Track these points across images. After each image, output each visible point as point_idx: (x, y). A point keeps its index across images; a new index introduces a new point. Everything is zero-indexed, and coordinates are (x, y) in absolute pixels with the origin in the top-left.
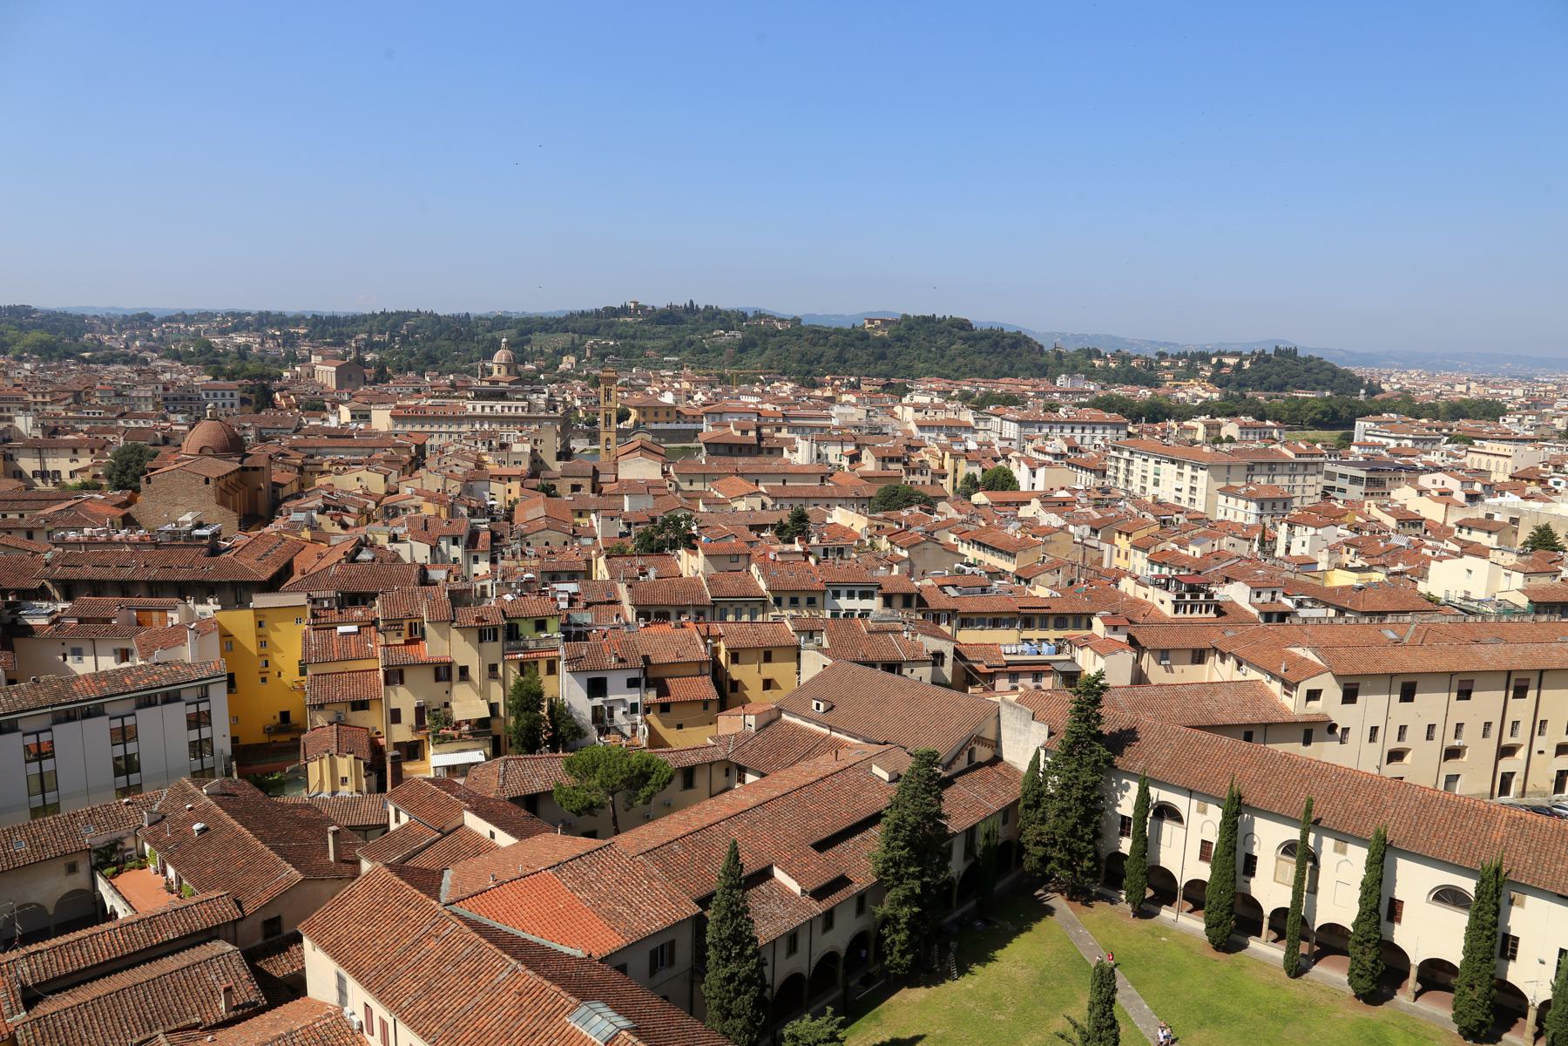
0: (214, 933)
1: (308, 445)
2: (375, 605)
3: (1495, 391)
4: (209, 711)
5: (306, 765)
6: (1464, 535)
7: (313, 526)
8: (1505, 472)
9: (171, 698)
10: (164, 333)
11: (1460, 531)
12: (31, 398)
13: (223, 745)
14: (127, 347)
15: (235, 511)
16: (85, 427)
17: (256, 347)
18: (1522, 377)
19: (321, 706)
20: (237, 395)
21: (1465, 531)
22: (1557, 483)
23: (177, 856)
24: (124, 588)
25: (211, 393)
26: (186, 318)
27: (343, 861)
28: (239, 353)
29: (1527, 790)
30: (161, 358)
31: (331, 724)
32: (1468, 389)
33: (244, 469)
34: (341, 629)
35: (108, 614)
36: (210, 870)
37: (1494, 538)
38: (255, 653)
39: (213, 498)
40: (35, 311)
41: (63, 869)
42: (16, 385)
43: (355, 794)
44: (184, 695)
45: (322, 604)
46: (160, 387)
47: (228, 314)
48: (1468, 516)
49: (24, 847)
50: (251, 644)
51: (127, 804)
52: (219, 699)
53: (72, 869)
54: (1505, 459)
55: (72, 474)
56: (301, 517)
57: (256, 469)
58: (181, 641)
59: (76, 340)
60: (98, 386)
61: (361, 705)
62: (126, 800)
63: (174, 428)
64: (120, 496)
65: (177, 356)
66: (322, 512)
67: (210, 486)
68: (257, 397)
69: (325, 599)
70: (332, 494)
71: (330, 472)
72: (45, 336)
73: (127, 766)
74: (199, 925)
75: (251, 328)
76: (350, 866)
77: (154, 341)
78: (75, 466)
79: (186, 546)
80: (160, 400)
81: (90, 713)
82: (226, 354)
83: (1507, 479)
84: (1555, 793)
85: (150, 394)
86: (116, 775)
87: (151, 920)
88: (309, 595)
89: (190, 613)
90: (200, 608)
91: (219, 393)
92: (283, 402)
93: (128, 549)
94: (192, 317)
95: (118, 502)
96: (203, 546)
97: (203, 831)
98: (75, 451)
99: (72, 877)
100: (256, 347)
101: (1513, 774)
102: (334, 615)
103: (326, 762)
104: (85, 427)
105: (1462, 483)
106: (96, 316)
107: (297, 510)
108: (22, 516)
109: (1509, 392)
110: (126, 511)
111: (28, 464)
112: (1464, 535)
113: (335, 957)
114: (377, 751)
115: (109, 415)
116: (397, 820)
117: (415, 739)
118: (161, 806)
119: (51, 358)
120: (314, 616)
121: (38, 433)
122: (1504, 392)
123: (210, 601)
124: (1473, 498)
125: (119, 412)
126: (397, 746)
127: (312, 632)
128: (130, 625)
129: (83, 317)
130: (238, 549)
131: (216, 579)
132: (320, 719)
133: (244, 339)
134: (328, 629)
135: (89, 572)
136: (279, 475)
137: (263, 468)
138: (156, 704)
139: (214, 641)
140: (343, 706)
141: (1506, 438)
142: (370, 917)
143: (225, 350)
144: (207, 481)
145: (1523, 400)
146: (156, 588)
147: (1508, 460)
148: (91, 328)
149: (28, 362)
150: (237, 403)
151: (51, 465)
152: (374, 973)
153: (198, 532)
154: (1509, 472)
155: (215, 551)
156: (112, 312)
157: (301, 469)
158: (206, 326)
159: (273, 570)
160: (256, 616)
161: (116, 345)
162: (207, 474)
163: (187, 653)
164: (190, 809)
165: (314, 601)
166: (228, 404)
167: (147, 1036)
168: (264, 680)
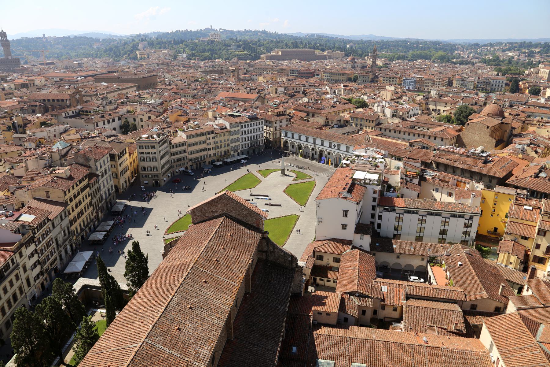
0: (456, 301)
1: (529, 111)
2: (541, 201)
4: (472, 224)
5: (499, 254)
7: (523, 151)
9: (461, 216)
10: (482, 50)
12: (436, 80)
13: (473, 235)
14: (468, 57)
15: (495, 139)
16: (451, 95)
17: (516, 58)
19: (510, 234)
20: (505, 82)
23: (451, 270)
24: (454, 170)
25: (495, 81)
26: (491, 45)
27: (503, 296)
28: (509, 61)
30: (480, 62)
31: (512, 241)
33: (502, 123)
34: (525, 207)
35: (448, 180)
36: (460, 280)
38: (491, 207)
39: (489, 134)
40: (441, 43)
41: (420, 259)
42: (432, 74)
43: (513, 269)
44: (465, 217)
45: (521, 195)
46: (477, 78)
47: (507, 43)
49: (413, 249)
50: (491, 204)
51: (441, 246)
52: (476, 222)
53: (423, 260)
55: (444, 111)
56: (520, 146)
57: (506, 124)
58: (468, 197)
59: (452, 54)
60: (457, 75)
61: (526, 238)
62: (441, 245)
63: (480, 99)
64: (458, 127)
65: (485, 62)
66: (529, 146)
67: (489, 129)
68: (512, 84)
69: (522, 194)
70: (534, 138)
71: (536, 125)
72: (443, 53)
73: (443, 232)
74: (453, 297)
75: (516, 49)
76: (505, 298)
77: (478, 54)
78: (445, 109)
79: (477, 158)
80: (476, 82)
81: (437, 215)
82: (504, 61)
85: (473, 81)
86: (440, 234)
87: (440, 290)
88: (516, 191)
89: (473, 186)
90: (477, 185)
91: (498, 81)
92: (523, 86)
93: (458, 156)
94: (494, 44)
95: (457, 129)
96: (482, 159)
97: (461, 265)
98: (446, 104)
99: (422, 262)
100: (516, 58)
102: (524, 201)
103: (506, 255)
104: (451, 95)
106: (460, 45)
107: (519, 144)
108: (428, 129)
110: (459, 133)
111: (432, 107)
113: (492, 336)
114: (527, 256)
115: (459, 91)
116: (527, 290)
117: (543, 257)
118: (450, 251)
119: (443, 62)
120: (516, 199)
121: (436, 96)
123: (481, 183)
125: (462, 90)
126: (535, 257)
127: (514, 205)
128: (454, 185)
129: (456, 45)
130: (495, 162)
131: (484, 173)
132: (509, 238)
133: (512, 54)
134: (520, 205)
135: (445, 161)
136: (517, 125)
137: (509, 124)
138: (456, 217)
139: (479, 199)
140: (518, 236)
142: (508, 329)
143: (503, 59)
144: (488, 127)
146: (464, 172)
148: (457, 49)
149: (436, 63)
150: (504, 85)
151: (438, 108)
152: (504, 350)
153: (481, 154)
155: (486, 162)
156: (465, 41)
157: (524, 122)
158: (498, 48)
159: (505, 173)
160: (495, 194)
161: (464, 56)
162: (488, 125)
163: (469, 202)
164: (459, 256)
165: (518, 194)
166: (500, 85)
167: (432, 325)
168: (492, 215)
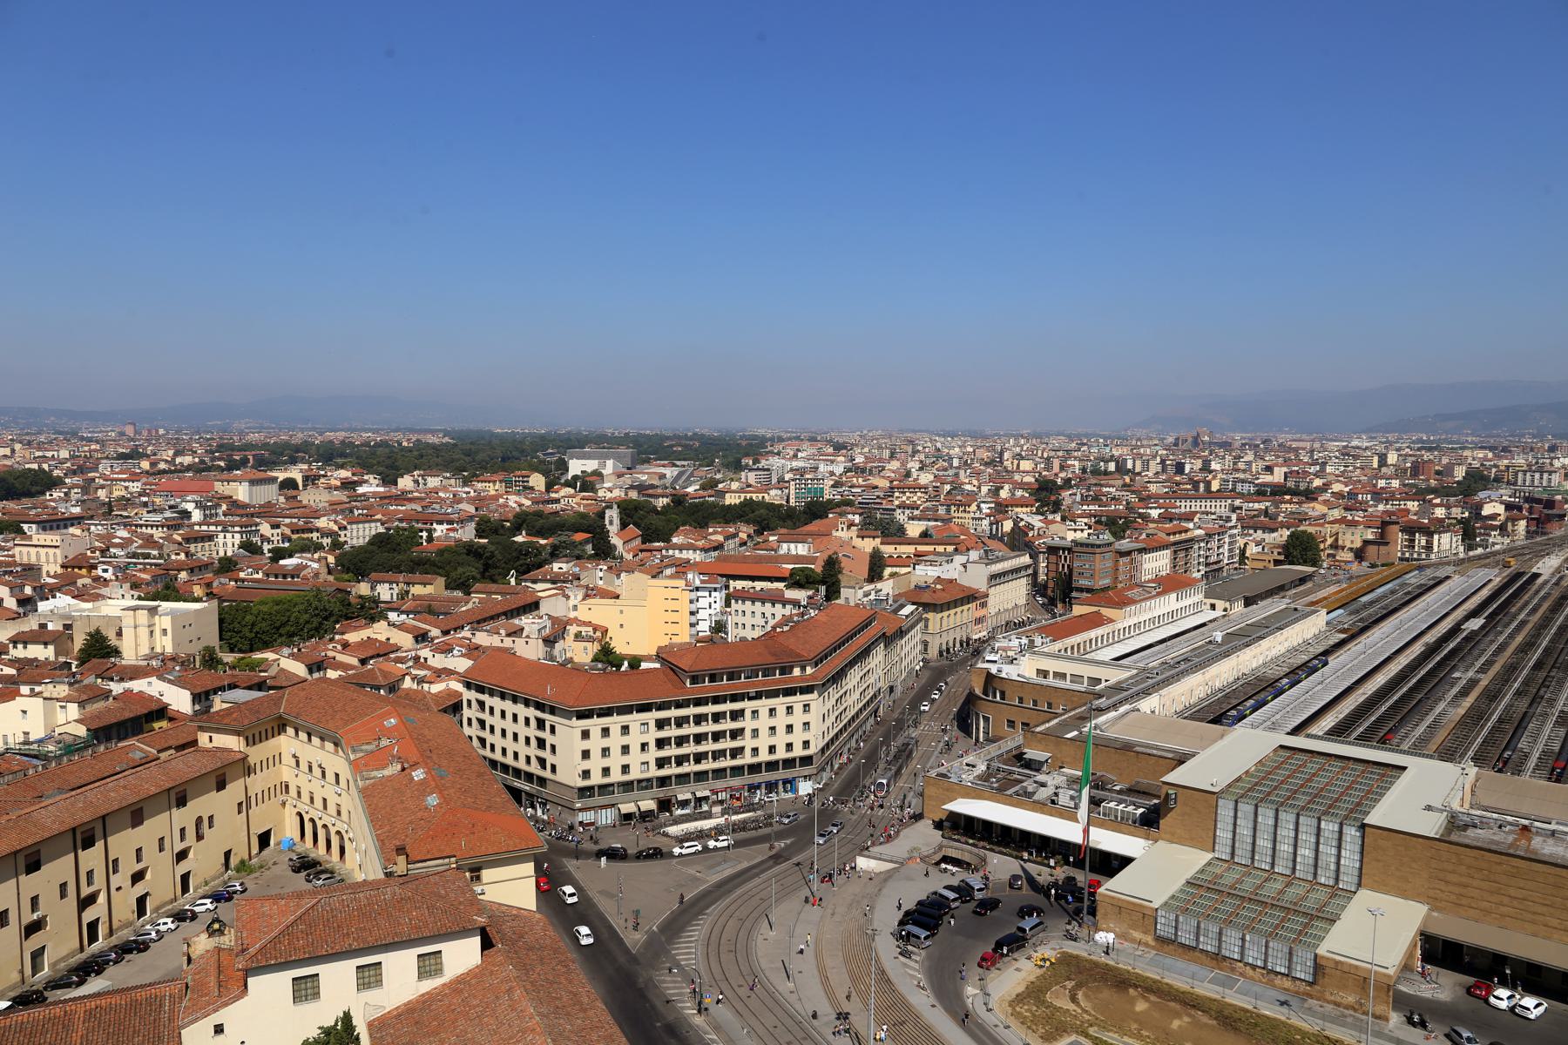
3: (40, 454)
6: (19, 652)
8: (55, 562)
11: (15, 647)
18: (67, 433)
21: (20, 646)
22: (105, 571)
29: (114, 927)
32: (13, 451)
37: (51, 648)
48: (22, 630)
54: (53, 550)
83: (60, 571)
84: (139, 918)
101: (98, 920)
105: (11, 588)
109: (55, 453)
112: (19, 652)
122: (49, 454)
124: (24, 602)
141: (55, 523)
145: (68, 465)
147: (57, 551)
154: (60, 561)
